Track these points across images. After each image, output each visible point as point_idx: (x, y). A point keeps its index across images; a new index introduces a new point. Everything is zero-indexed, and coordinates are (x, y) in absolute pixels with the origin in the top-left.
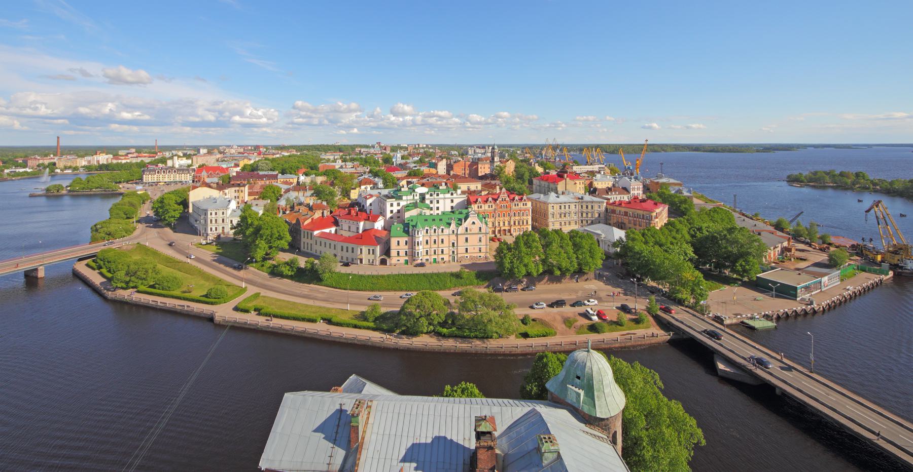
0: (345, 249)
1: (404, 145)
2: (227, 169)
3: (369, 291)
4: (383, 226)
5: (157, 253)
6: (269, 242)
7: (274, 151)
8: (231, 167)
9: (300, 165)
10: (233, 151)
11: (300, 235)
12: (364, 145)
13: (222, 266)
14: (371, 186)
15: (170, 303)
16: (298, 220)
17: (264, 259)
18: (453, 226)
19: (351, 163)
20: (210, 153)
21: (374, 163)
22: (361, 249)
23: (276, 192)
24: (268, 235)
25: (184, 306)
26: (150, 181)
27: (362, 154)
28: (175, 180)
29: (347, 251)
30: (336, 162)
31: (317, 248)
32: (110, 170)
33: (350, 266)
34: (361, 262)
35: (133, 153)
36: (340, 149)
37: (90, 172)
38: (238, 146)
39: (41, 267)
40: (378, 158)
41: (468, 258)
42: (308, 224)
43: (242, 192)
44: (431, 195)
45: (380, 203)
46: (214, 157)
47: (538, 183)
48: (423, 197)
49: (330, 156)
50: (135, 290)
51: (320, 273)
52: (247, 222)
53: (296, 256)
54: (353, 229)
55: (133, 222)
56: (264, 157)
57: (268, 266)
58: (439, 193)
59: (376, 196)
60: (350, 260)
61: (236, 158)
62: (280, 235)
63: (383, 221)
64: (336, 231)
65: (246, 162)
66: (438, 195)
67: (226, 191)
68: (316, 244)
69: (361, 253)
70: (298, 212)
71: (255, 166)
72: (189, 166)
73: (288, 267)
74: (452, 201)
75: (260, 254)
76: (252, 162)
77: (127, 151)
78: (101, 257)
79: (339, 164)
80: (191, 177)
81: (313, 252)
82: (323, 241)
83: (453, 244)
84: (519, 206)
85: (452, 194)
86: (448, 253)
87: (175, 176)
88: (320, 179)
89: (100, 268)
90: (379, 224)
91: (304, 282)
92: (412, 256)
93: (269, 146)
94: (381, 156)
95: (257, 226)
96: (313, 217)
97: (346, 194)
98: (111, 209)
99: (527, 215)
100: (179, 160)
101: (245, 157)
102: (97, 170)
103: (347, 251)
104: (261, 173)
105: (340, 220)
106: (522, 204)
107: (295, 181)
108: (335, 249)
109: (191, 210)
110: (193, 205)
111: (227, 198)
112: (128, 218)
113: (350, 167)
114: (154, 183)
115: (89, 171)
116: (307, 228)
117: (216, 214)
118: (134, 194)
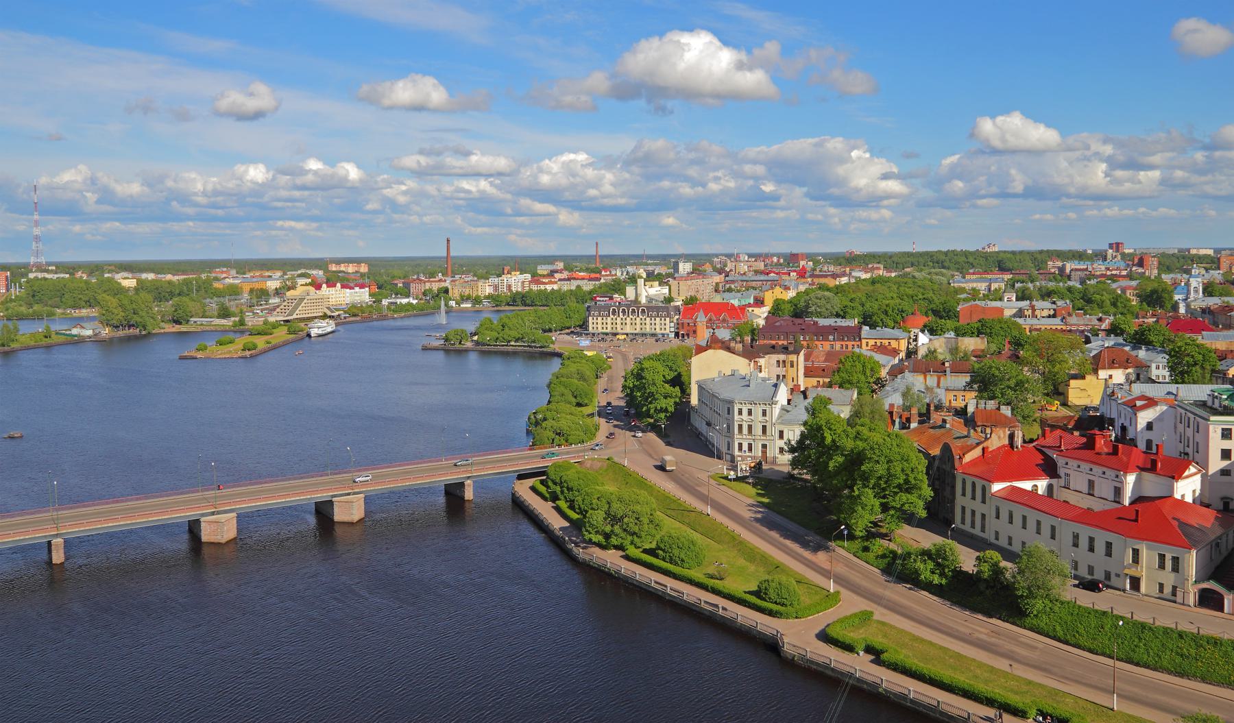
0: (1084, 542)
1: (1203, 252)
2: (743, 308)
3: (1170, 672)
4: (1197, 494)
5: (646, 484)
6: (881, 493)
7: (832, 268)
8: (750, 305)
9: (906, 305)
10: (743, 268)
12: (1070, 251)
13: (775, 535)
14: (1130, 370)
15: (691, 594)
16: (946, 449)
17: (870, 536)
19: (1047, 304)
20: (697, 272)
21: (1114, 304)
22: (1136, 553)
23: (868, 373)
24: (880, 478)
25: (717, 606)
26: (600, 330)
27: (1069, 277)
28: (643, 331)
29: (1091, 549)
30: (1001, 299)
31: (998, 529)
32: (529, 306)
33: (1100, 590)
34: (1135, 584)
35: (560, 271)
36: (1001, 263)
37: (499, 308)
38: (750, 256)
39: (469, 481)
40: (1124, 290)
42: (973, 462)
43: (792, 366)
45: (1181, 427)
46: (710, 280)
49: (973, 281)
50: (621, 553)
51: (1020, 593)
52: (824, 438)
53: (950, 541)
54: (1104, 489)
55: (592, 415)
56: (813, 284)
57: (880, 553)
59: (1165, 401)
60: (1099, 575)
61: (754, 284)
62: (907, 481)
63: (1197, 479)
64: (1050, 487)
65: (778, 293)
67: (762, 361)
68: (998, 517)
69: (1136, 559)
70: (941, 427)
71: (802, 304)
72: (669, 300)
73: (931, 565)
75: (861, 521)
76: (791, 294)
77: (551, 267)
78: (554, 477)
79: (1010, 306)
80: (672, 325)
81: (989, 536)
82: (1019, 511)
87: (643, 322)
88: (970, 344)
89: (554, 498)
90: (1187, 488)
91: (975, 609)
93: (819, 255)
94: (1134, 283)
95: (852, 450)
96: (985, 445)
97: (1058, 392)
98: (550, 383)
100: (647, 287)
101: (774, 284)
102: (508, 305)
103: (1091, 549)
104: (823, 322)
105: (1060, 461)
107: (903, 345)
108: (1053, 537)
109: (694, 400)
110: (701, 388)
111: (764, 380)
112: (579, 405)
113: (1045, 313)
114: (607, 334)
115: (497, 306)
116: (971, 471)
117: (750, 413)
118: (579, 355)
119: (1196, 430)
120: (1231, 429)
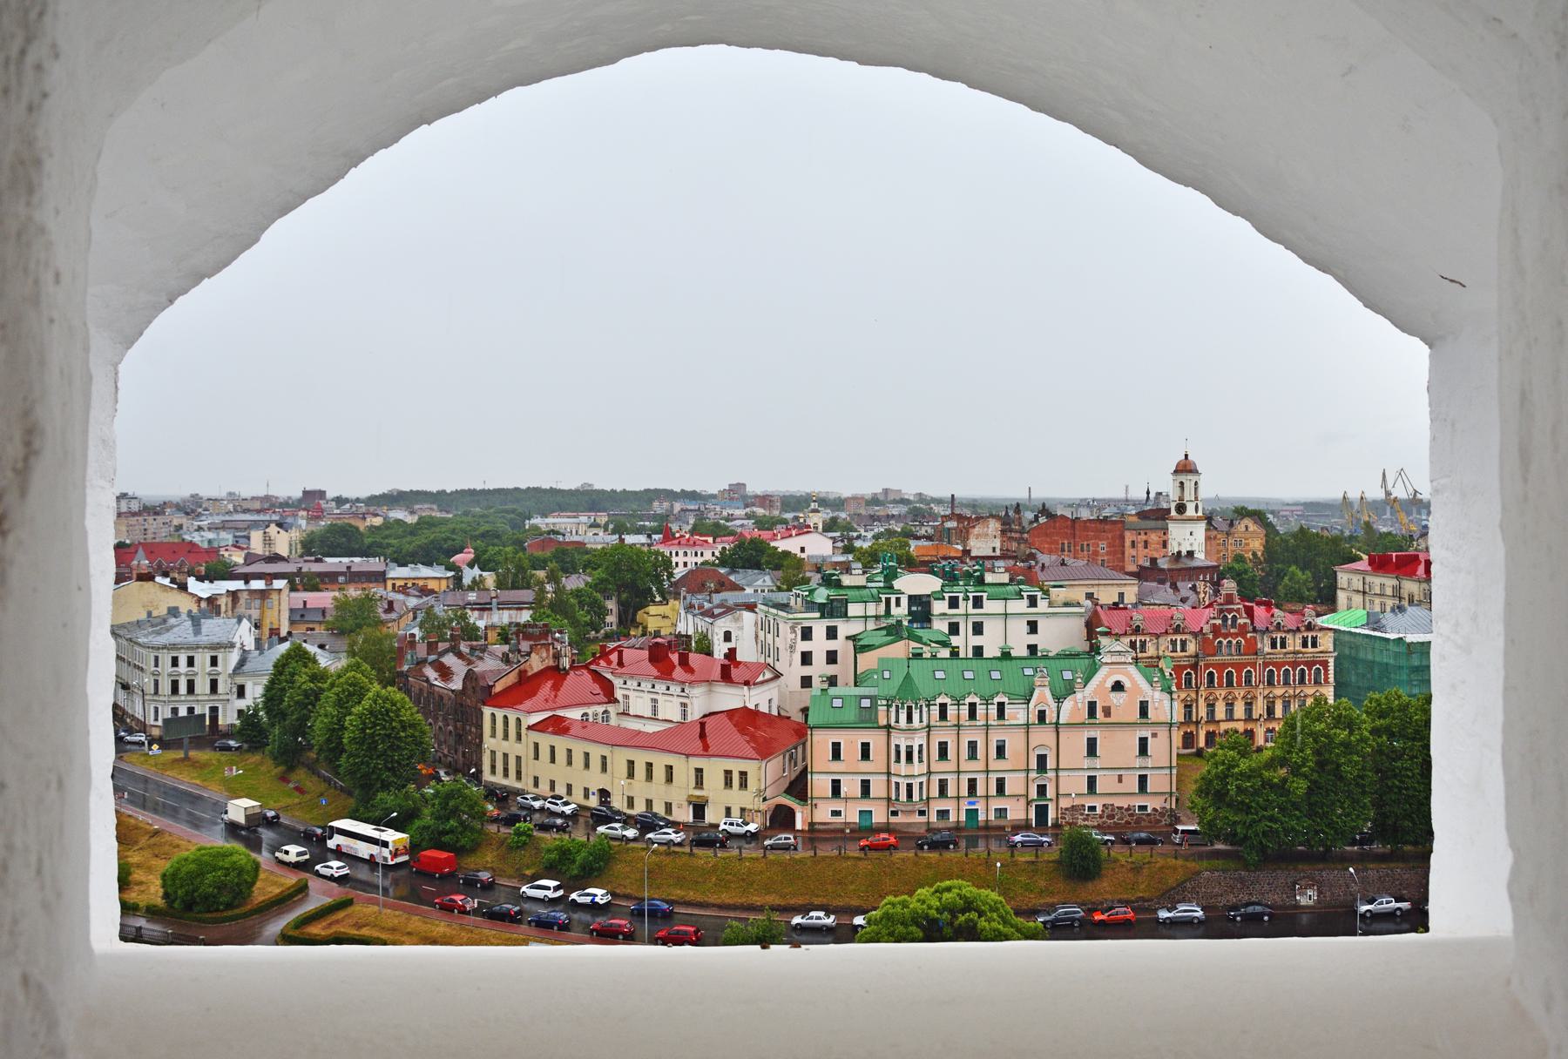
0: (640, 771)
11: (480, 727)
18: (1043, 696)
29: (649, 775)
41: (1099, 811)
44: (954, 603)
45: (761, 634)
47: (1357, 583)
48: (921, 608)
58: (985, 595)
66: (978, 603)
68: (537, 757)
74: (1033, 627)
83: (1042, 760)
84: (1290, 648)
85: (1033, 602)
86: (1024, 792)
92: (889, 799)
99: (1317, 682)
103: (649, 775)
105: (617, 682)
106: (1299, 641)
108: (604, 769)
119: (776, 634)
120: (811, 628)
